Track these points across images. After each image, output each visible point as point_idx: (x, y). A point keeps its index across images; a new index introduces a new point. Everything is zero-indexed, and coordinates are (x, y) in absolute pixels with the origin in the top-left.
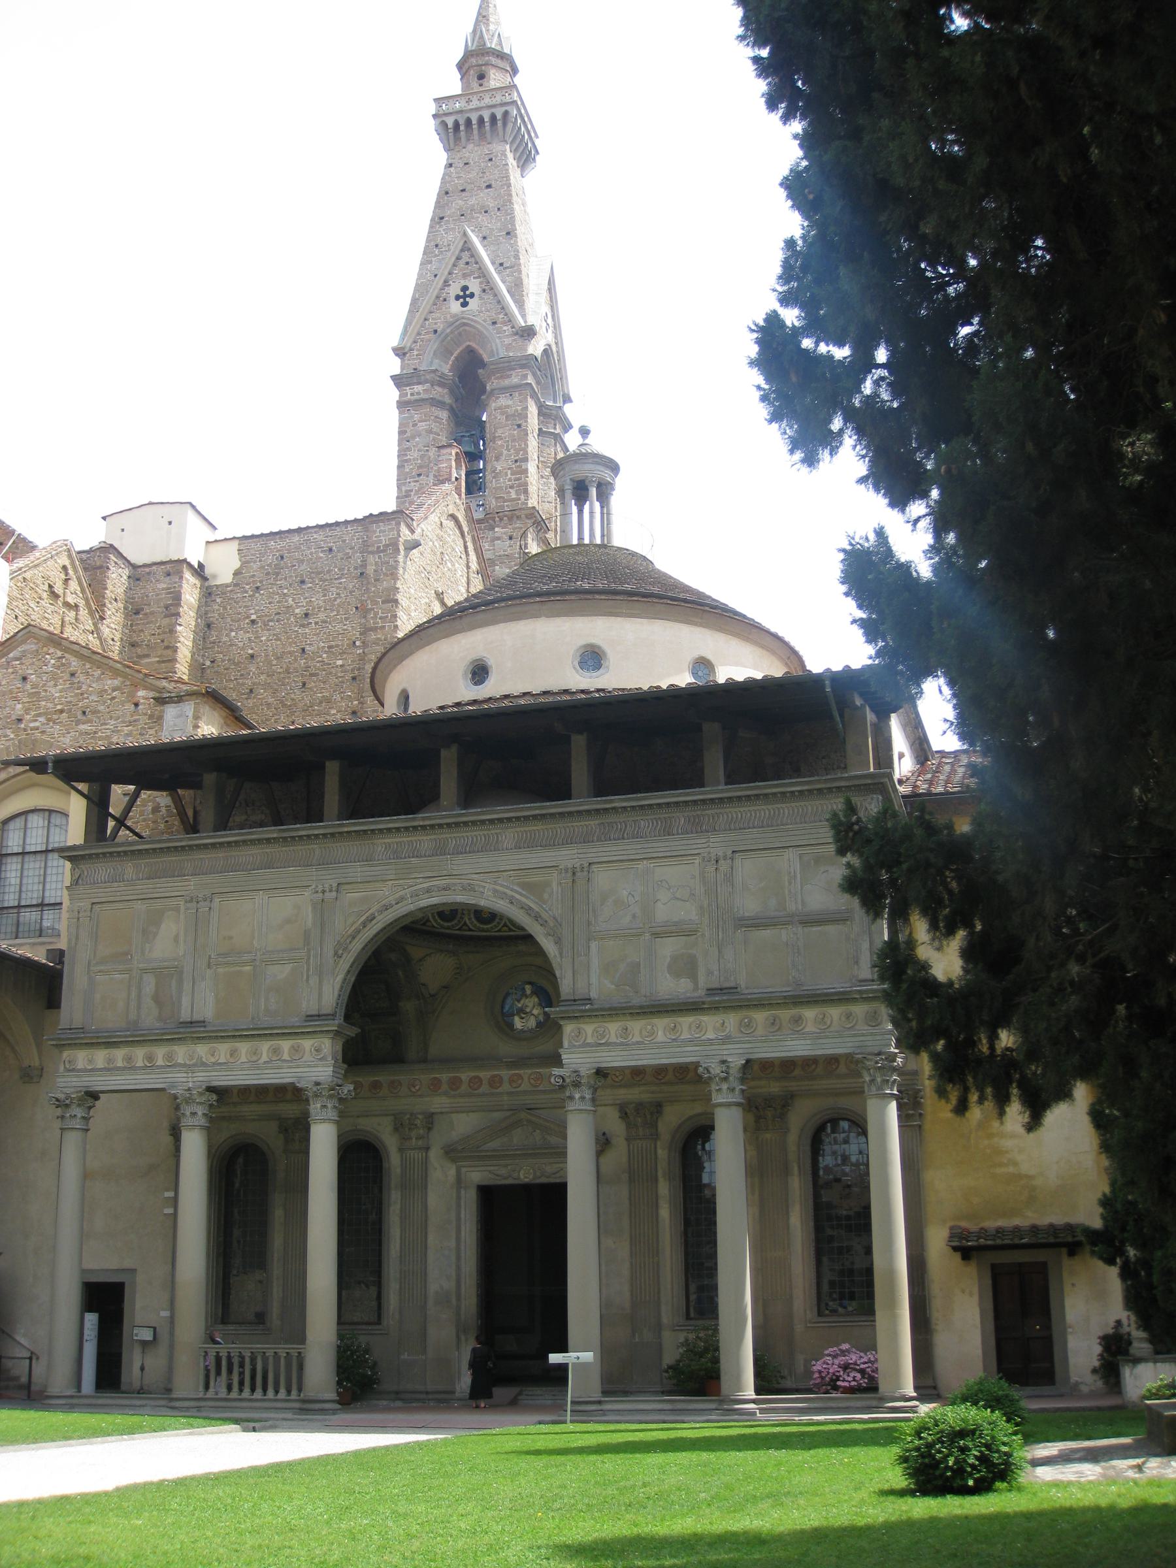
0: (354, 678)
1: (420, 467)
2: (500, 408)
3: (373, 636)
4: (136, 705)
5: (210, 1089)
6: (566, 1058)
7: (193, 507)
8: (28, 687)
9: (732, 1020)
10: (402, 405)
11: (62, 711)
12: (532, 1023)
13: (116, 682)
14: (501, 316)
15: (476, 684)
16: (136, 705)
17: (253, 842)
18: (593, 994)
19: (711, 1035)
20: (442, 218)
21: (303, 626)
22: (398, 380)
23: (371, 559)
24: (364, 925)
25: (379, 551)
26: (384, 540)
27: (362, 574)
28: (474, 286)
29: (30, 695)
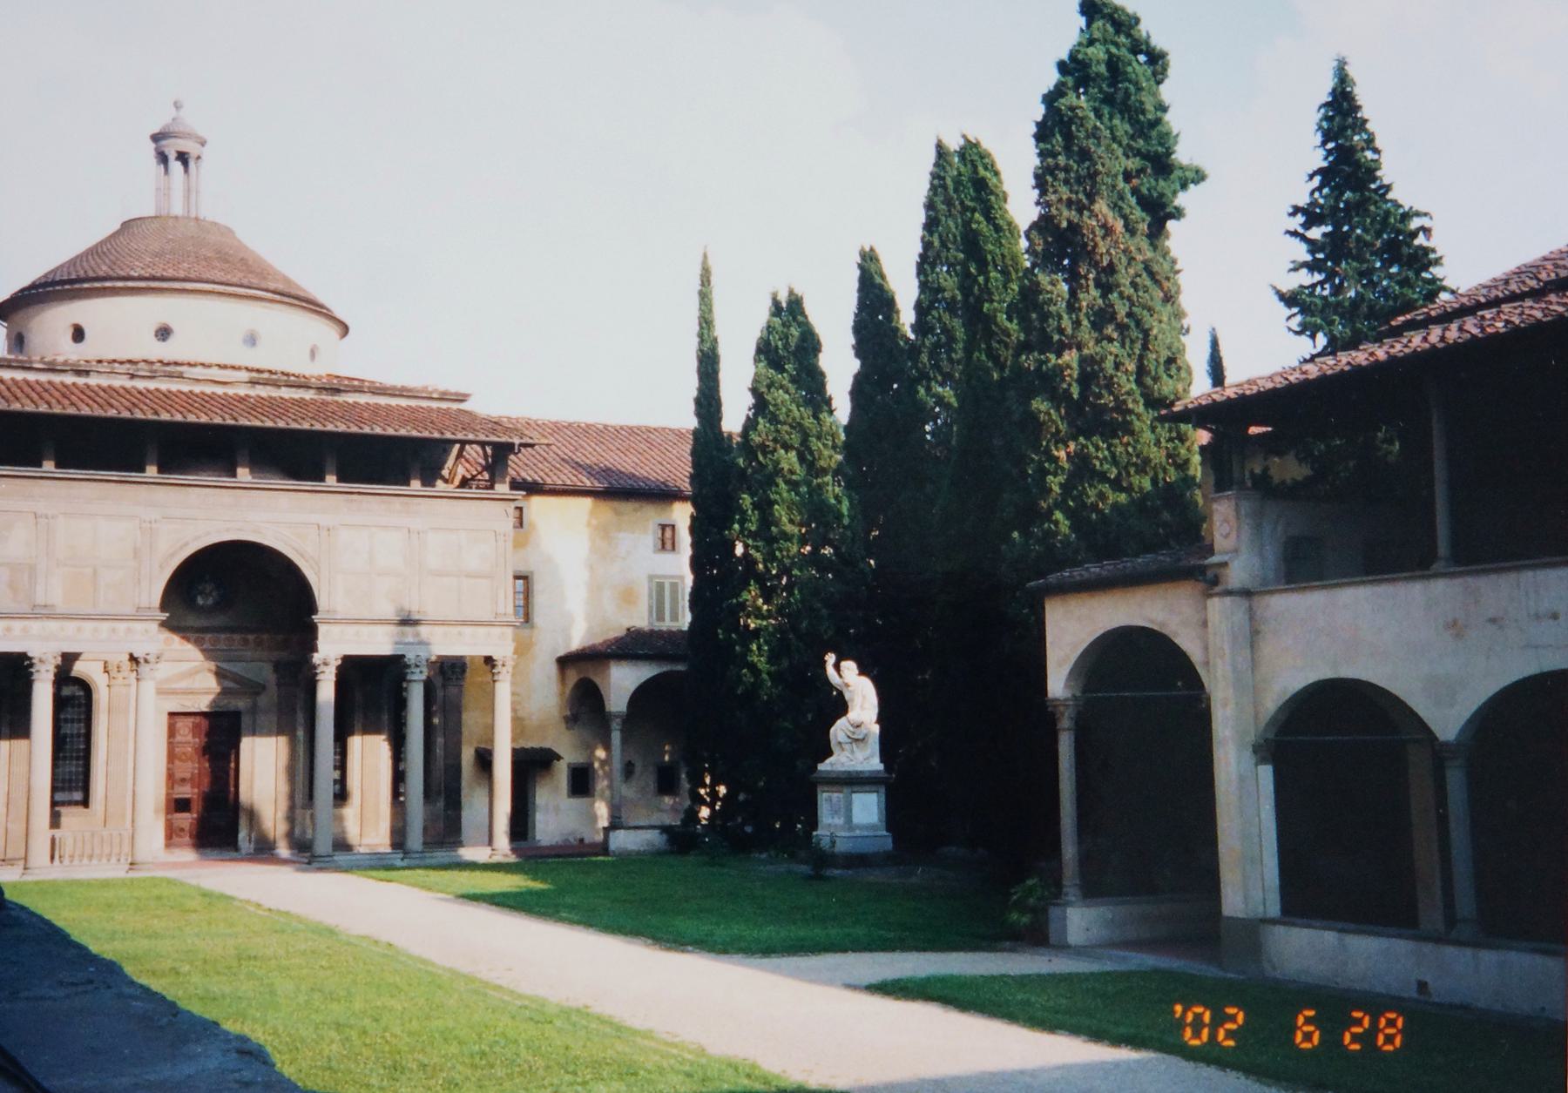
12: (210, 601)
19: (410, 639)
24: (181, 548)
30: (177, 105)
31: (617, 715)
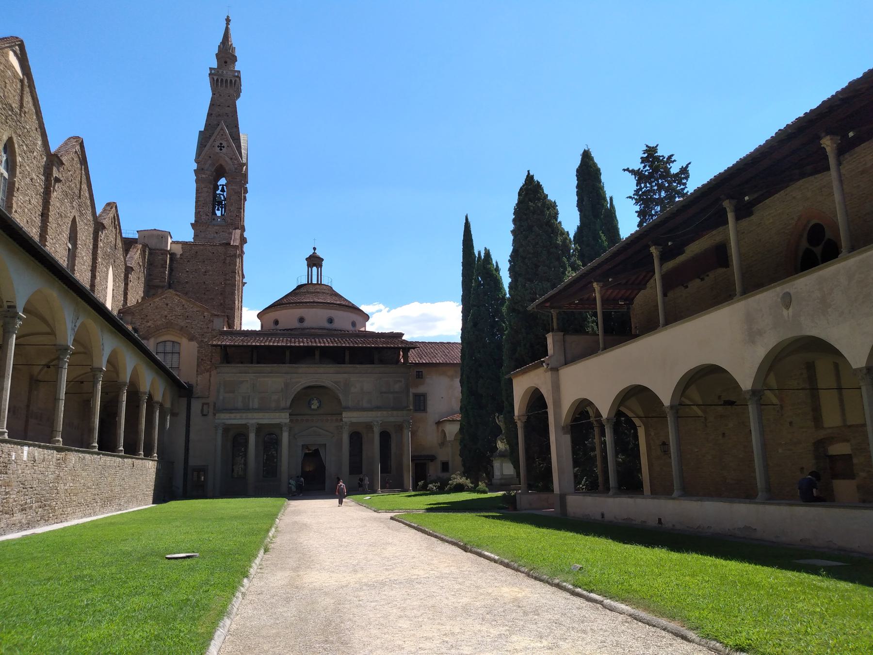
0: (221, 294)
1: (204, 204)
2: (233, 189)
3: (228, 282)
4: (204, 317)
5: (258, 424)
6: (343, 420)
7: (170, 233)
8: (169, 307)
9: (379, 413)
10: (197, 181)
11: (180, 315)
12: (316, 407)
13: (199, 309)
14: (234, 157)
15: (301, 322)
16: (204, 317)
17: (268, 367)
18: (350, 406)
20: (212, 114)
21: (204, 275)
22: (196, 172)
23: (228, 258)
25: (230, 256)
26: (232, 253)
27: (224, 262)
28: (225, 144)
29: (169, 309)
30: (315, 249)
31: (450, 441)
